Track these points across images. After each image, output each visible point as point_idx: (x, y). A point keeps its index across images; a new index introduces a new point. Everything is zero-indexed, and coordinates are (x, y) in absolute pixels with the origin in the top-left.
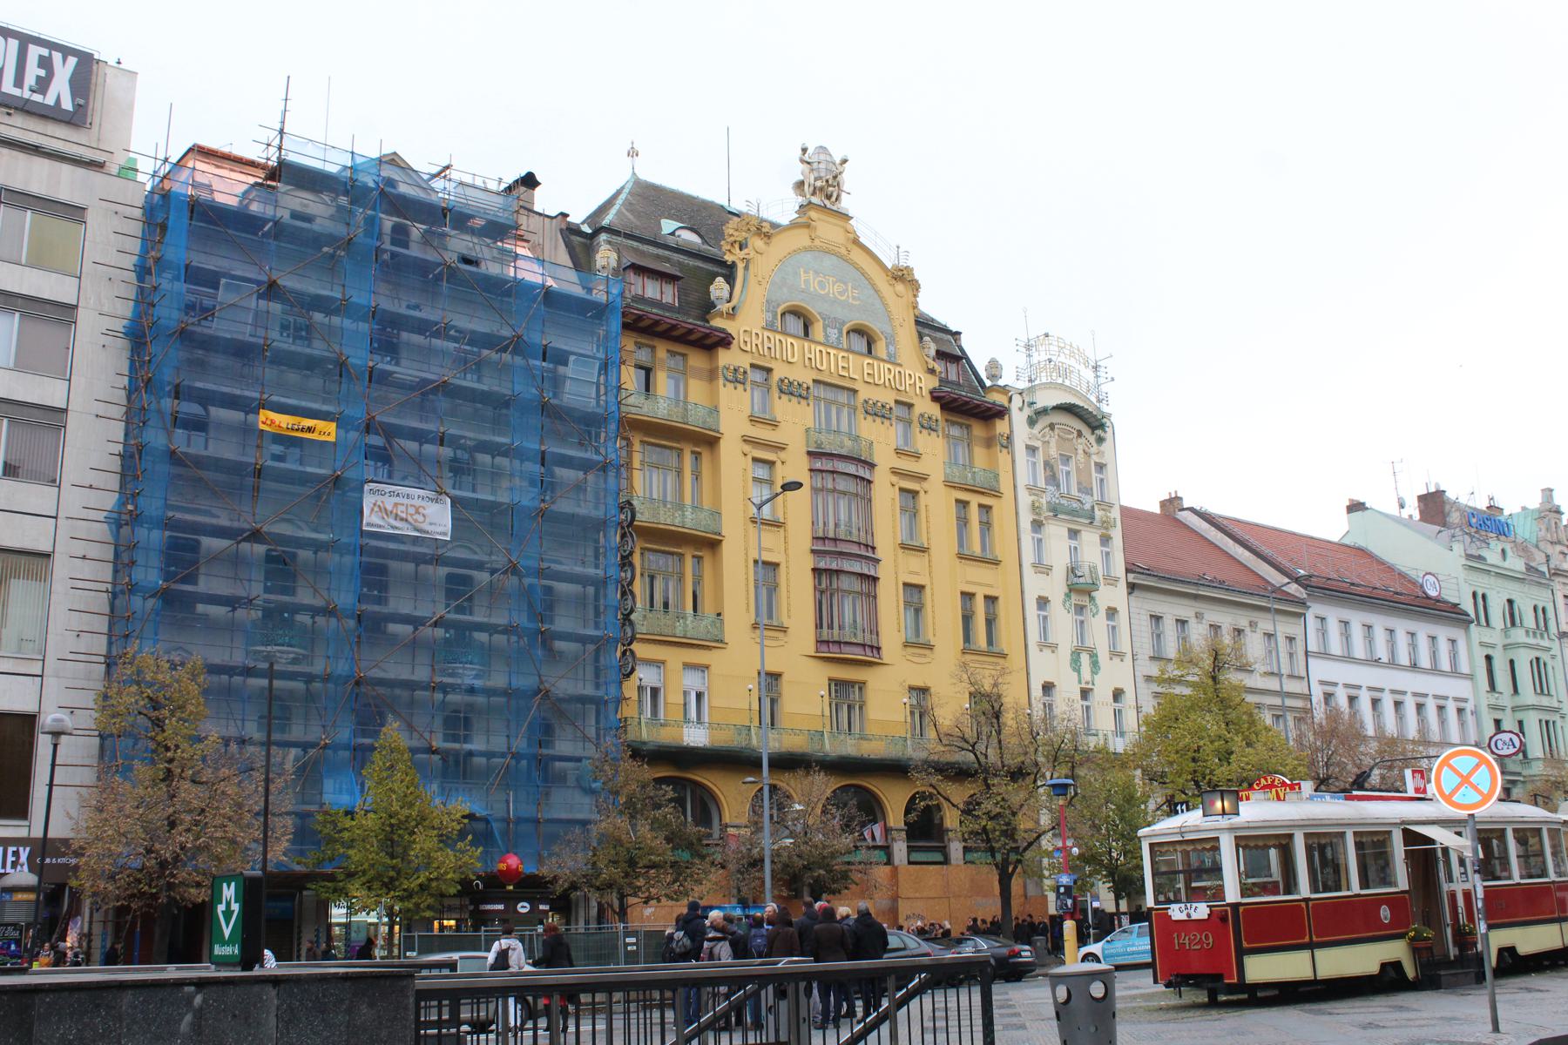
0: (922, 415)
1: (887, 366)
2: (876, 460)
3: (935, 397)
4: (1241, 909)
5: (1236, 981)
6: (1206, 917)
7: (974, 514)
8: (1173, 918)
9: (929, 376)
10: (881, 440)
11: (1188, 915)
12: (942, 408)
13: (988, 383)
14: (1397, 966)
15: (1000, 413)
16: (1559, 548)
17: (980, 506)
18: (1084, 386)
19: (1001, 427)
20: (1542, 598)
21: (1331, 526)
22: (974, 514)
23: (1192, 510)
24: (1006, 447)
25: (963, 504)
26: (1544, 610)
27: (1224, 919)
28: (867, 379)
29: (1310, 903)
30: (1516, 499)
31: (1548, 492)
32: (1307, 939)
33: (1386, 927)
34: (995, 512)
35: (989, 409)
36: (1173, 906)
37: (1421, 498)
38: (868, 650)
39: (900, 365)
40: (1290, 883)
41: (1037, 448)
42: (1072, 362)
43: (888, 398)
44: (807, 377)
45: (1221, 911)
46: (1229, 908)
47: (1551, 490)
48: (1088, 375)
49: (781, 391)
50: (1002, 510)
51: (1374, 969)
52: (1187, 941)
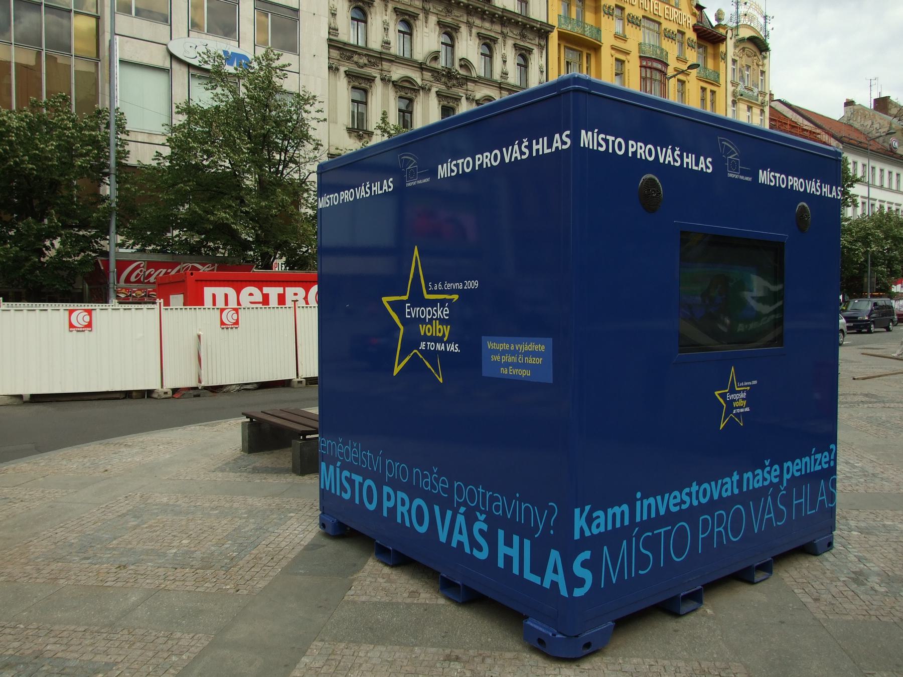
0: (689, 39)
1: (675, 10)
2: (669, 62)
3: (696, 29)
7: (708, 93)
9: (693, 17)
10: (671, 49)
12: (698, 37)
13: (714, 23)
15: (722, 39)
17: (711, 91)
18: (759, 27)
19: (722, 48)
22: (708, 93)
24: (724, 59)
25: (703, 89)
28: (666, 17)
34: (717, 93)
35: (719, 37)
39: (680, 10)
41: (737, 61)
42: (755, 13)
43: (674, 28)
44: (639, 13)
48: (762, 21)
49: (629, 21)
50: (720, 92)
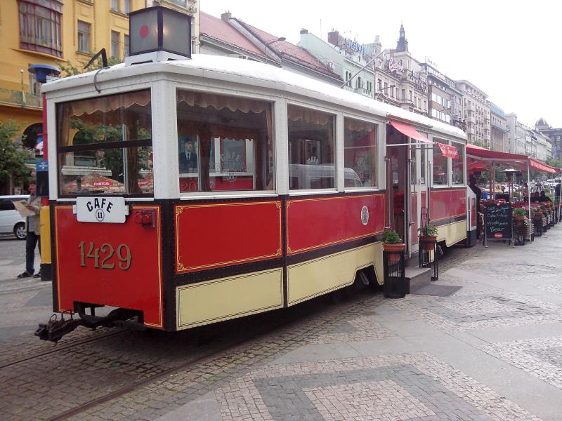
4: (179, 210)
5: (160, 326)
6: (123, 220)
8: (80, 219)
11: (100, 215)
14: (368, 272)
16: (379, 60)
20: (370, 78)
21: (294, 39)
23: (235, 19)
26: (370, 83)
27: (147, 225)
29: (288, 203)
30: (364, 39)
31: (377, 38)
32: (279, 253)
33: (366, 229)
36: (79, 200)
37: (329, 34)
38: (54, 53)
40: (264, 177)
45: (144, 213)
46: (158, 208)
47: (379, 36)
51: (348, 279)
52: (96, 256)
